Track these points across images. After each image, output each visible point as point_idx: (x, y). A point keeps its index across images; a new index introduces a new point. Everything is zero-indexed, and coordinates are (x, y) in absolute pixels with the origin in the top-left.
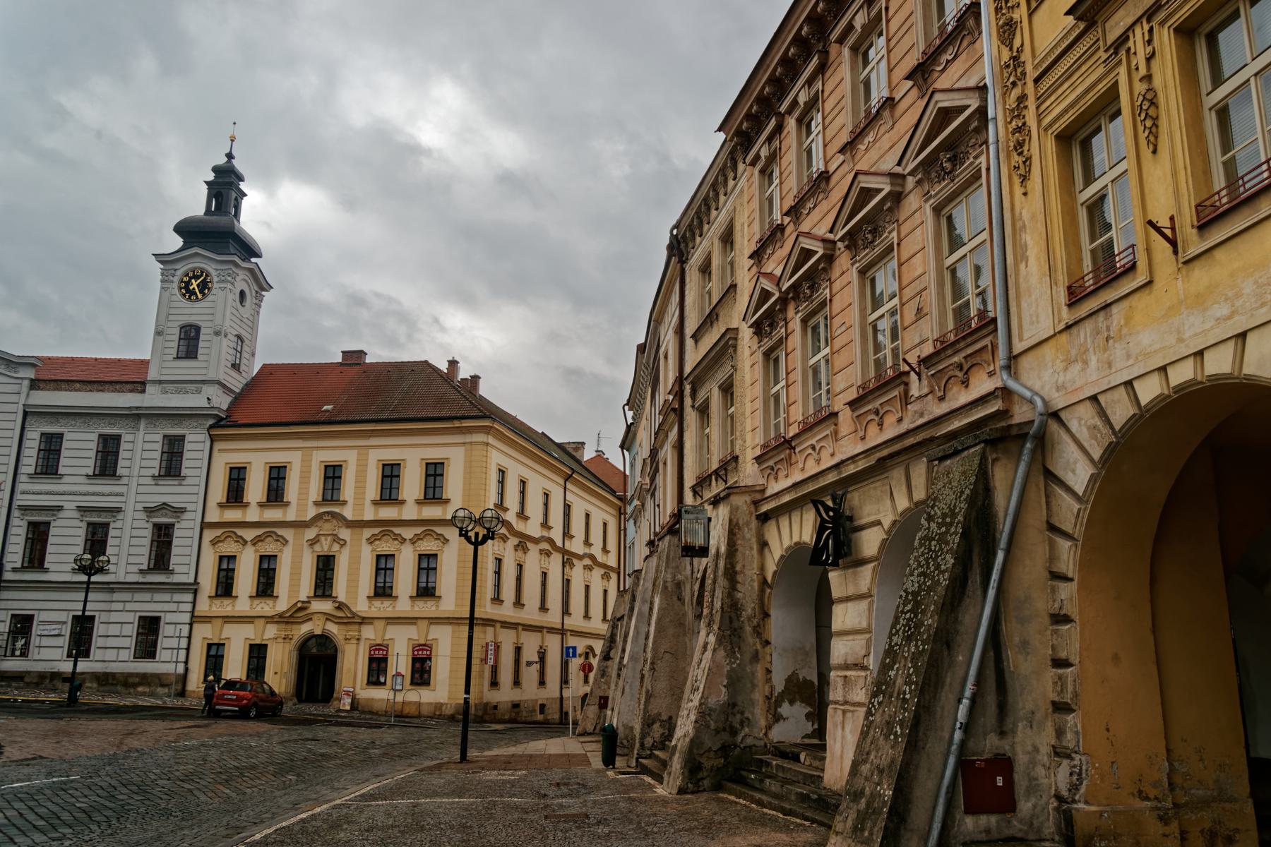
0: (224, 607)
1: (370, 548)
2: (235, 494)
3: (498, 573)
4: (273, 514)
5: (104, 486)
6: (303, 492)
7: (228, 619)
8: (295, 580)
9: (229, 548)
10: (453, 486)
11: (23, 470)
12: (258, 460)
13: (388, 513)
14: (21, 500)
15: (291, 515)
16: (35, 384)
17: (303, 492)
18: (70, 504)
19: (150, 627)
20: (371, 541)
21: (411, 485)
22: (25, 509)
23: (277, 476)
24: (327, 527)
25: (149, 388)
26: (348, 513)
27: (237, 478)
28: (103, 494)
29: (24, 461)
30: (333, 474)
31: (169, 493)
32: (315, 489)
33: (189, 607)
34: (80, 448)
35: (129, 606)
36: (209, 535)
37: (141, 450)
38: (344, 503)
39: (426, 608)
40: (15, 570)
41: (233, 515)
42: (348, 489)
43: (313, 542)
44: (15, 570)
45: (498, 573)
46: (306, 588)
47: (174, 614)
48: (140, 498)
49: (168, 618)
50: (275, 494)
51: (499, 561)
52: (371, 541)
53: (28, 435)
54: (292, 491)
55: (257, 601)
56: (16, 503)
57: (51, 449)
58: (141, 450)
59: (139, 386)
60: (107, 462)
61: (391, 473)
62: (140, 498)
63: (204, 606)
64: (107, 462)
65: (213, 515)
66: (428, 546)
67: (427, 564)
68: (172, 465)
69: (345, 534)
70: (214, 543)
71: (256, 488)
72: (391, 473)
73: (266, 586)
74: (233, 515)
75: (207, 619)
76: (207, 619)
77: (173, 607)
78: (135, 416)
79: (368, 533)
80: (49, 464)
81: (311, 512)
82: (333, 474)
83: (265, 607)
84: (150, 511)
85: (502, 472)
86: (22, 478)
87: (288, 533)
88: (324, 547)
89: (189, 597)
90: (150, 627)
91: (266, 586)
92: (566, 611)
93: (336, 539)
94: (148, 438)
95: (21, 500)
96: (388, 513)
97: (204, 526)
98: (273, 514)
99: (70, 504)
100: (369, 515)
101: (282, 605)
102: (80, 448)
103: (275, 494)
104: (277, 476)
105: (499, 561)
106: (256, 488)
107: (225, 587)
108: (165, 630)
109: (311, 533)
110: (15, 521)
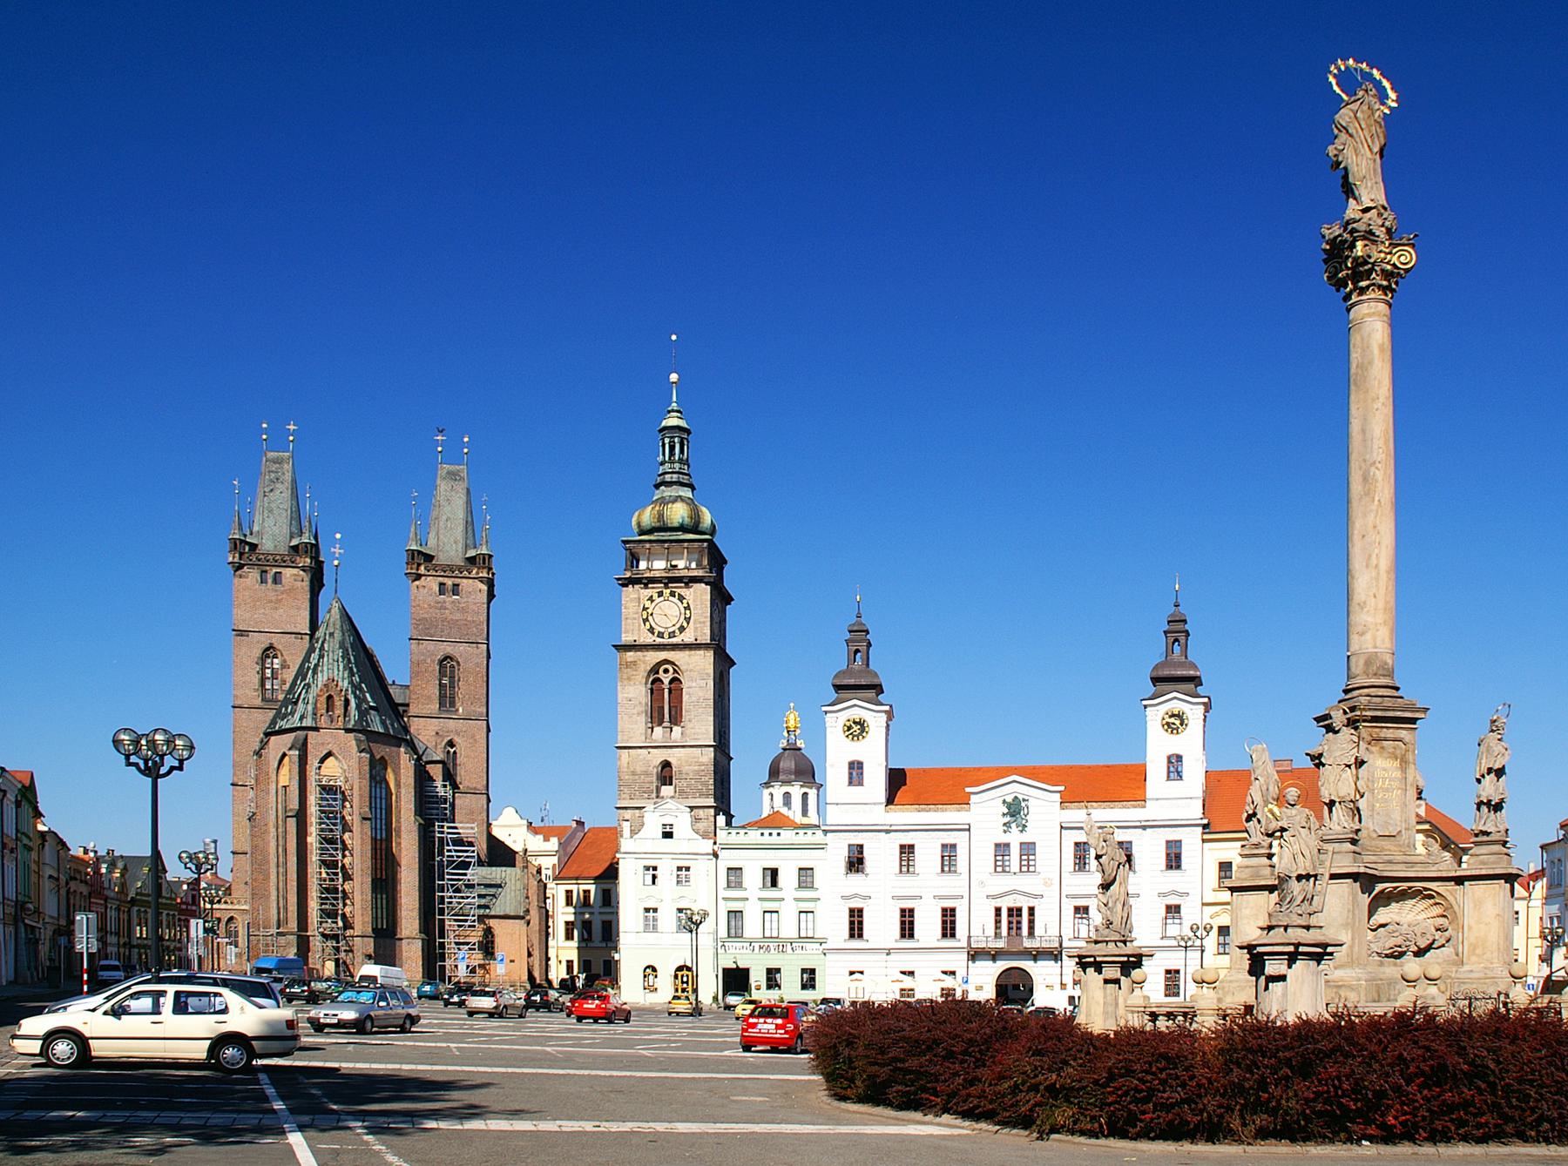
16: (1066, 801)
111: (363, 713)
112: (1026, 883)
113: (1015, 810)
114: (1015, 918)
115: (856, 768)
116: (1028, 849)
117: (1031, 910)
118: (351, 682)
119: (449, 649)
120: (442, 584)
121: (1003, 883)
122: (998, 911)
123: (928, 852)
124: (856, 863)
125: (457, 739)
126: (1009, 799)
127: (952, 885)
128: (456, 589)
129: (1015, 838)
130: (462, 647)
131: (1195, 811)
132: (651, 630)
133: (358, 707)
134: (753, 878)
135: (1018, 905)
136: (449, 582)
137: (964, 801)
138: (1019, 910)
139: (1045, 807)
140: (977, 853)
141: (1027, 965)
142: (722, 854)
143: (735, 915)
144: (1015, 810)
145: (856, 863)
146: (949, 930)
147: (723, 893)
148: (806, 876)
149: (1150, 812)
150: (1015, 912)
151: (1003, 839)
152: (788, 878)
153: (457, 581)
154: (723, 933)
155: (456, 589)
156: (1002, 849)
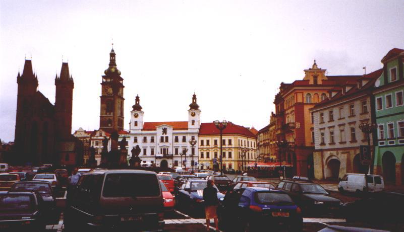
0: (203, 159)
4: (208, 147)
5: (184, 143)
7: (204, 161)
9: (202, 151)
10: (233, 142)
12: (205, 139)
14: (174, 145)
15: (210, 147)
16: (173, 129)
17: (212, 144)
18: (180, 146)
22: (175, 147)
23: (208, 141)
24: (216, 148)
27: (202, 142)
32: (213, 144)
34: (180, 138)
36: (200, 150)
37: (189, 138)
39: (230, 159)
46: (213, 157)
54: (210, 143)
59: (187, 129)
63: (200, 159)
65: (200, 147)
66: (230, 151)
67: (230, 154)
71: (205, 143)
73: (208, 156)
74: (202, 147)
75: (201, 161)
76: (201, 161)
78: (187, 133)
80: (177, 140)
81: (213, 146)
83: (208, 159)
87: (210, 149)
88: (216, 151)
91: (208, 156)
92: (249, 158)
93: (217, 150)
95: (174, 145)
97: (199, 148)
99: (180, 146)
101: (210, 159)
102: (180, 138)
104: (208, 141)
106: (205, 143)
107: (202, 156)
109: (213, 149)
112: (167, 144)
113: (165, 131)
114: (164, 151)
116: (167, 138)
122: (161, 149)
123: (149, 138)
124: (136, 141)
127: (153, 144)
129: (164, 136)
131: (197, 130)
132: (107, 94)
137: (155, 130)
139: (170, 132)
140: (157, 139)
144: (165, 131)
145: (136, 141)
146: (152, 153)
149: (189, 131)
150: (164, 149)
156: (162, 138)
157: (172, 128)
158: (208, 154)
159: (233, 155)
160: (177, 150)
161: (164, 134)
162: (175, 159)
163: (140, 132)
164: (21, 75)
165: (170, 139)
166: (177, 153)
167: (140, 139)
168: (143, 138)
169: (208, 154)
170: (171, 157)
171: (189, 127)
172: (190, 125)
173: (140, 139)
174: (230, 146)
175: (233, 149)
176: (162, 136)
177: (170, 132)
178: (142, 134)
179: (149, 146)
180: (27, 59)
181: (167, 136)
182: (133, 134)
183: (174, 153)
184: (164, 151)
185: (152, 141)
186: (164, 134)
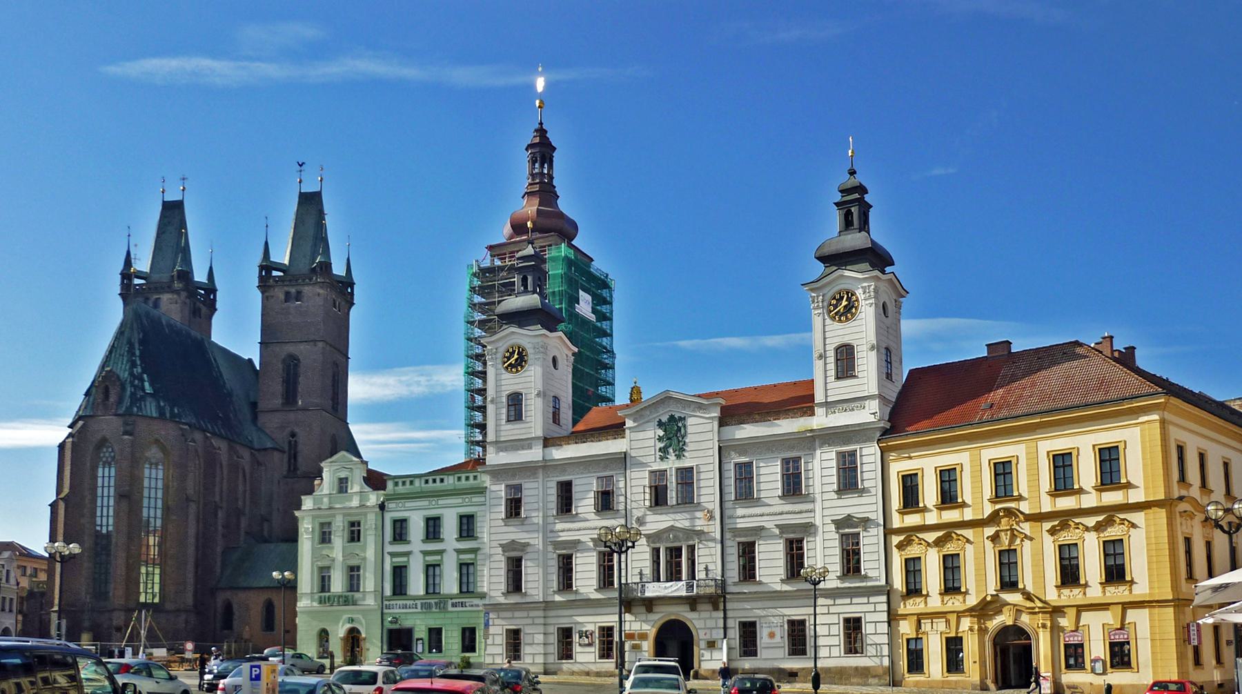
1: (1052, 538)
2: (911, 498)
3: (1189, 552)
4: (951, 516)
6: (977, 494)
8: (981, 577)
11: (726, 498)
12: (927, 466)
13: (1066, 503)
15: (968, 515)
17: (977, 494)
19: (853, 627)
20: (1052, 532)
21: (1087, 472)
23: (948, 479)
25: (819, 411)
26: (1025, 507)
28: (792, 513)
29: (726, 490)
30: (1003, 471)
31: (854, 506)
33: (885, 607)
34: (769, 476)
35: (833, 610)
36: (896, 540)
37: (822, 468)
38: (1020, 498)
40: (735, 584)
41: (913, 520)
42: (1022, 484)
43: (995, 538)
44: (735, 584)
45: (1189, 552)
46: (992, 586)
47: (873, 614)
48: (826, 512)
49: (869, 617)
50: (948, 498)
51: (1188, 540)
52: (1052, 532)
53: (726, 467)
54: (966, 491)
55: (946, 598)
56: (726, 527)
57: (745, 475)
58: (822, 468)
60: (793, 486)
61: (1062, 464)
62: (826, 512)
64: (793, 486)
65: (896, 522)
66: (1113, 532)
68: (848, 481)
69: (1026, 527)
70: (900, 546)
71: (930, 493)
72: (1062, 464)
74: (913, 520)
77: (871, 608)
79: (1047, 525)
81: (988, 509)
82: (1003, 471)
83: (955, 603)
84: (839, 524)
85: (1181, 449)
86: (728, 505)
87: (968, 533)
89: (884, 598)
90: (853, 627)
94: (825, 456)
96: (1066, 503)
98: (951, 516)
100: (1047, 505)
101: (972, 601)
102: (769, 476)
103: (948, 498)
104: (948, 479)
105: (1188, 540)
106: (930, 493)
108: (868, 629)
109: (990, 531)
110: (728, 543)
111: (135, 400)
113: (673, 434)
114: (673, 558)
115: (515, 403)
116: (686, 476)
117: (692, 549)
118: (132, 374)
119: (290, 349)
120: (287, 294)
121: (658, 522)
122: (656, 552)
124: (514, 508)
125: (297, 430)
126: (665, 419)
128: (299, 296)
129: (672, 464)
130: (302, 347)
133: (133, 394)
134: (416, 529)
135: (676, 544)
136: (293, 290)
138: (680, 549)
140: (634, 489)
141: (683, 614)
142: (391, 505)
143: (399, 573)
145: (514, 508)
147: (390, 548)
148: (467, 526)
149: (820, 420)
151: (663, 466)
152: (450, 528)
153: (299, 288)
154: (388, 591)
155: (299, 296)
157: (716, 413)
158: (951, 566)
159: (1138, 563)
160: (748, 553)
161: (672, 457)
162: (740, 612)
163: (535, 454)
164: (143, 264)
165: (708, 491)
166: (748, 572)
167: (539, 496)
168: (553, 492)
169: (951, 566)
170: (717, 599)
171: (819, 397)
172: (826, 385)
173: (539, 496)
174: (1113, 498)
175: (1138, 517)
176: (655, 467)
177: (702, 431)
178: (546, 466)
179: (586, 538)
180: (168, 198)
181: (686, 463)
182: (499, 472)
183: (733, 574)
184: (673, 558)
185: (605, 501)
186: (672, 457)
